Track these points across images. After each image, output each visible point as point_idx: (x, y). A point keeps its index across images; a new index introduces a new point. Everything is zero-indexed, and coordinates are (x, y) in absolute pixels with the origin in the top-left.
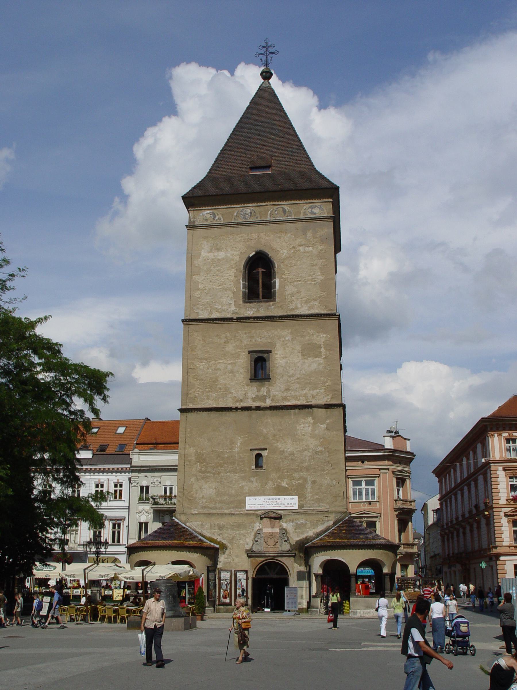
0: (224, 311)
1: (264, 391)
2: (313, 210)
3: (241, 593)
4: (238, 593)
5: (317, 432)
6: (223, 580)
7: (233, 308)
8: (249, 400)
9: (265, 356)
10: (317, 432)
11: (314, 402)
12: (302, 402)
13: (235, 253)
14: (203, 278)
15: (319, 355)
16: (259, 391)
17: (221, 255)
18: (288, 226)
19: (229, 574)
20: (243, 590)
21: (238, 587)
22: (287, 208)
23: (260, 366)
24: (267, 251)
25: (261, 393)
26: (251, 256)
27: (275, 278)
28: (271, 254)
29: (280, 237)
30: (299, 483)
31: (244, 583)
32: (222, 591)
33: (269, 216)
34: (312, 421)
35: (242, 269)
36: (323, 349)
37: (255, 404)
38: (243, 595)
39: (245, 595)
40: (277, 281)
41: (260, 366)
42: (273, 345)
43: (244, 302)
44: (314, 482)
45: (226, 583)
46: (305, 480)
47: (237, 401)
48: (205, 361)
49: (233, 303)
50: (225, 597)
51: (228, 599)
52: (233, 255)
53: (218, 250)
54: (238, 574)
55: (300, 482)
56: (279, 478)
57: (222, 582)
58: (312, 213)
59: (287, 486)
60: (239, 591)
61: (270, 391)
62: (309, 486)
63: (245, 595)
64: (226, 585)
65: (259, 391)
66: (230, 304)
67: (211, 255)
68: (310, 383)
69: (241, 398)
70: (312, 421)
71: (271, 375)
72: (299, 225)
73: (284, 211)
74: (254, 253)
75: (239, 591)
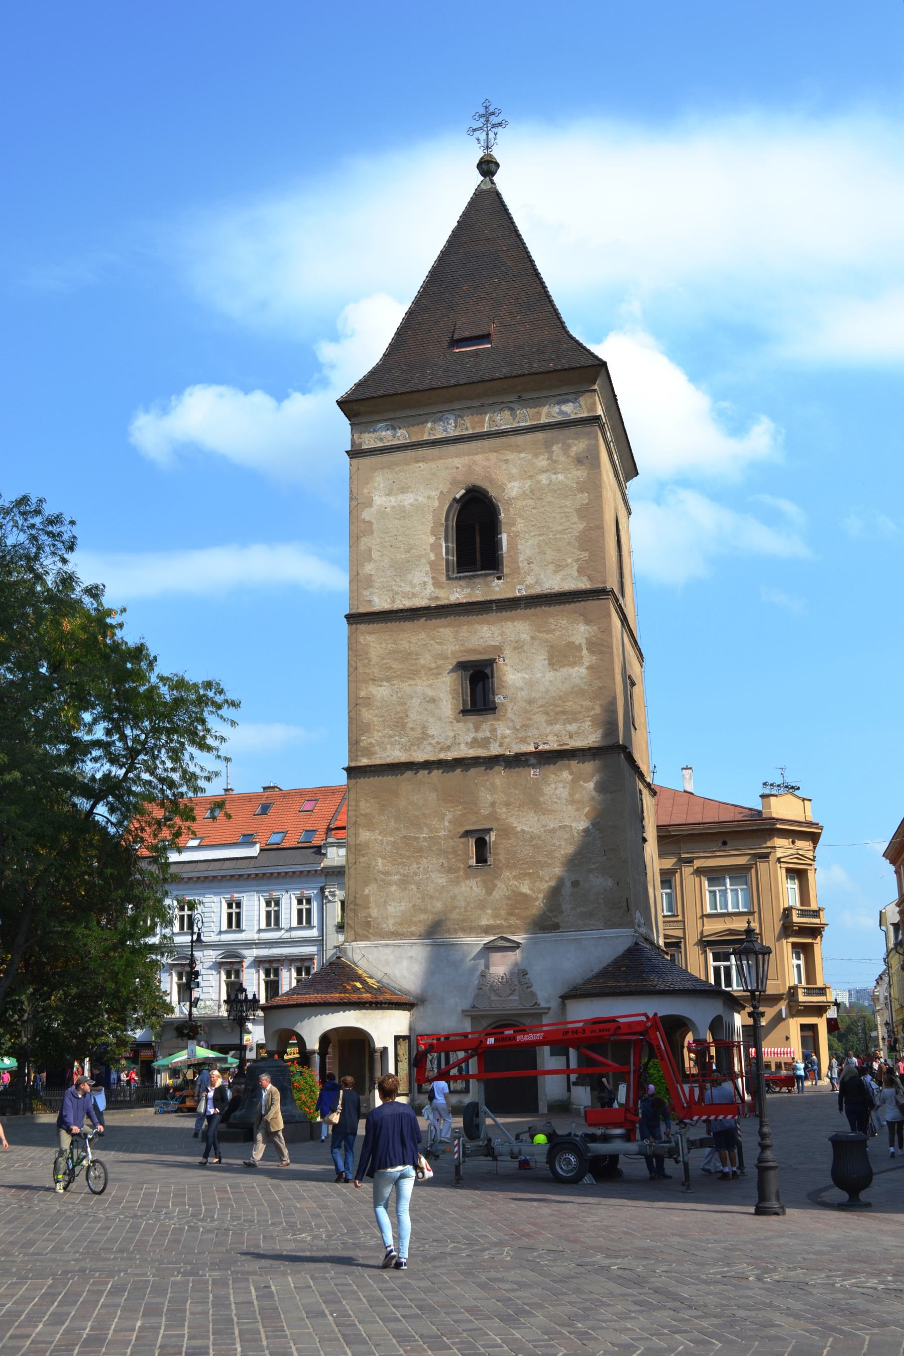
1: (485, 732)
5: (577, 796)
7: (430, 588)
8: (463, 746)
10: (577, 796)
14: (378, 540)
16: (477, 729)
17: (408, 499)
18: (520, 439)
23: (479, 686)
24: (485, 485)
25: (480, 735)
26: (458, 496)
27: (501, 533)
28: (492, 492)
29: (506, 461)
33: (486, 425)
34: (570, 777)
35: (443, 521)
36: (585, 652)
37: (472, 753)
40: (504, 537)
41: (479, 686)
42: (499, 649)
43: (449, 578)
47: (442, 749)
48: (385, 684)
49: (431, 581)
52: (429, 498)
53: (403, 490)
58: (561, 412)
61: (495, 730)
65: (477, 729)
66: (425, 583)
69: (448, 743)
70: (570, 777)
71: (499, 699)
72: (540, 435)
74: (463, 491)
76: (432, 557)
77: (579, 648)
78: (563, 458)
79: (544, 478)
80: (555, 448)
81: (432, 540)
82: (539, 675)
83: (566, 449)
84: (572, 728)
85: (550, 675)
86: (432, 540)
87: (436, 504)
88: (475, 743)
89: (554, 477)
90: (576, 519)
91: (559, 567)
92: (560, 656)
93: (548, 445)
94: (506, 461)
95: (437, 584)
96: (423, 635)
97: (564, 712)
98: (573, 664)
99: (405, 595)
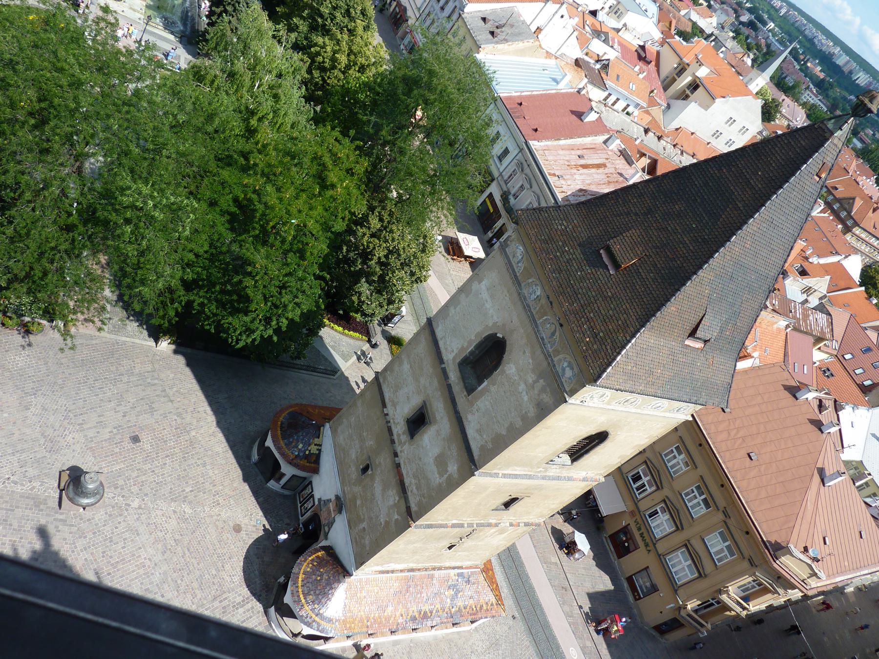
0: (446, 349)
2: (567, 369)
9: (427, 420)
11: (409, 494)
12: (407, 481)
13: (495, 318)
15: (441, 475)
16: (403, 433)
22: (557, 334)
36: (446, 476)
49: (454, 354)
53: (492, 296)
58: (564, 370)
67: (485, 295)
68: (419, 480)
73: (553, 334)
76: (466, 344)
77: (447, 471)
78: (536, 392)
79: (522, 387)
80: (541, 381)
81: (473, 338)
82: (430, 455)
83: (543, 390)
84: (415, 490)
85: (432, 461)
86: (473, 338)
87: (491, 324)
88: (399, 435)
89: (524, 393)
90: (506, 425)
91: (479, 431)
92: (441, 462)
93: (540, 376)
94: (524, 352)
95: (454, 358)
96: (431, 370)
97: (419, 480)
98: (439, 473)
99: (445, 343)
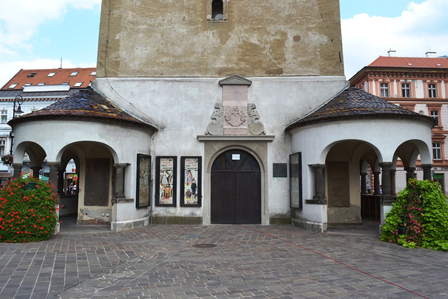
3: (191, 191)
4: (186, 191)
6: (163, 172)
19: (172, 162)
20: (194, 186)
21: (186, 182)
30: (275, 40)
31: (195, 174)
32: (161, 187)
38: (194, 193)
39: (196, 193)
44: (297, 38)
45: (167, 176)
46: (284, 34)
50: (166, 196)
51: (171, 198)
54: (187, 163)
55: (278, 37)
56: (246, 31)
57: (161, 174)
59: (257, 43)
60: (188, 188)
62: (290, 42)
63: (196, 193)
64: (168, 179)
75: (188, 188)
